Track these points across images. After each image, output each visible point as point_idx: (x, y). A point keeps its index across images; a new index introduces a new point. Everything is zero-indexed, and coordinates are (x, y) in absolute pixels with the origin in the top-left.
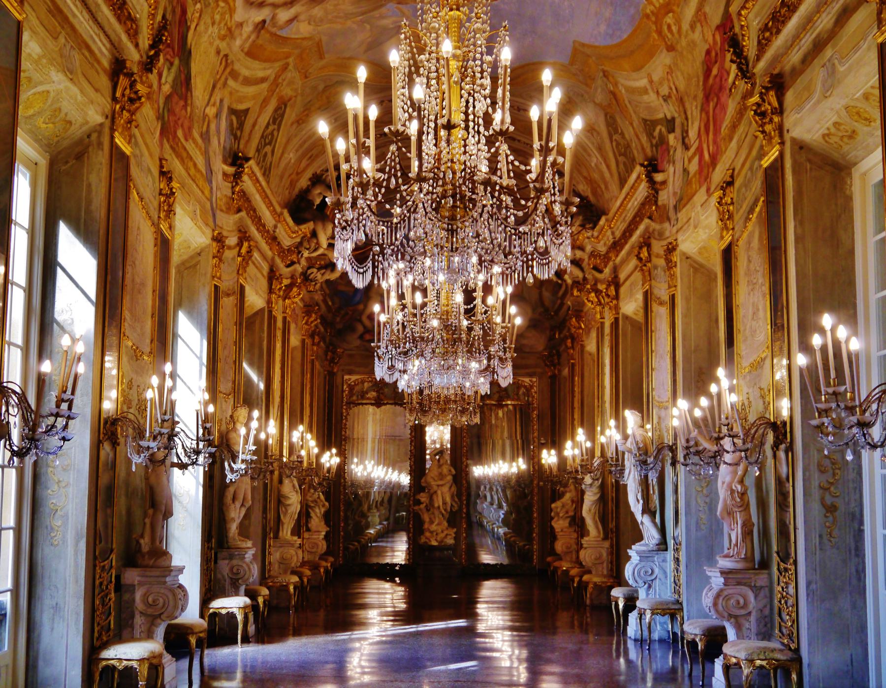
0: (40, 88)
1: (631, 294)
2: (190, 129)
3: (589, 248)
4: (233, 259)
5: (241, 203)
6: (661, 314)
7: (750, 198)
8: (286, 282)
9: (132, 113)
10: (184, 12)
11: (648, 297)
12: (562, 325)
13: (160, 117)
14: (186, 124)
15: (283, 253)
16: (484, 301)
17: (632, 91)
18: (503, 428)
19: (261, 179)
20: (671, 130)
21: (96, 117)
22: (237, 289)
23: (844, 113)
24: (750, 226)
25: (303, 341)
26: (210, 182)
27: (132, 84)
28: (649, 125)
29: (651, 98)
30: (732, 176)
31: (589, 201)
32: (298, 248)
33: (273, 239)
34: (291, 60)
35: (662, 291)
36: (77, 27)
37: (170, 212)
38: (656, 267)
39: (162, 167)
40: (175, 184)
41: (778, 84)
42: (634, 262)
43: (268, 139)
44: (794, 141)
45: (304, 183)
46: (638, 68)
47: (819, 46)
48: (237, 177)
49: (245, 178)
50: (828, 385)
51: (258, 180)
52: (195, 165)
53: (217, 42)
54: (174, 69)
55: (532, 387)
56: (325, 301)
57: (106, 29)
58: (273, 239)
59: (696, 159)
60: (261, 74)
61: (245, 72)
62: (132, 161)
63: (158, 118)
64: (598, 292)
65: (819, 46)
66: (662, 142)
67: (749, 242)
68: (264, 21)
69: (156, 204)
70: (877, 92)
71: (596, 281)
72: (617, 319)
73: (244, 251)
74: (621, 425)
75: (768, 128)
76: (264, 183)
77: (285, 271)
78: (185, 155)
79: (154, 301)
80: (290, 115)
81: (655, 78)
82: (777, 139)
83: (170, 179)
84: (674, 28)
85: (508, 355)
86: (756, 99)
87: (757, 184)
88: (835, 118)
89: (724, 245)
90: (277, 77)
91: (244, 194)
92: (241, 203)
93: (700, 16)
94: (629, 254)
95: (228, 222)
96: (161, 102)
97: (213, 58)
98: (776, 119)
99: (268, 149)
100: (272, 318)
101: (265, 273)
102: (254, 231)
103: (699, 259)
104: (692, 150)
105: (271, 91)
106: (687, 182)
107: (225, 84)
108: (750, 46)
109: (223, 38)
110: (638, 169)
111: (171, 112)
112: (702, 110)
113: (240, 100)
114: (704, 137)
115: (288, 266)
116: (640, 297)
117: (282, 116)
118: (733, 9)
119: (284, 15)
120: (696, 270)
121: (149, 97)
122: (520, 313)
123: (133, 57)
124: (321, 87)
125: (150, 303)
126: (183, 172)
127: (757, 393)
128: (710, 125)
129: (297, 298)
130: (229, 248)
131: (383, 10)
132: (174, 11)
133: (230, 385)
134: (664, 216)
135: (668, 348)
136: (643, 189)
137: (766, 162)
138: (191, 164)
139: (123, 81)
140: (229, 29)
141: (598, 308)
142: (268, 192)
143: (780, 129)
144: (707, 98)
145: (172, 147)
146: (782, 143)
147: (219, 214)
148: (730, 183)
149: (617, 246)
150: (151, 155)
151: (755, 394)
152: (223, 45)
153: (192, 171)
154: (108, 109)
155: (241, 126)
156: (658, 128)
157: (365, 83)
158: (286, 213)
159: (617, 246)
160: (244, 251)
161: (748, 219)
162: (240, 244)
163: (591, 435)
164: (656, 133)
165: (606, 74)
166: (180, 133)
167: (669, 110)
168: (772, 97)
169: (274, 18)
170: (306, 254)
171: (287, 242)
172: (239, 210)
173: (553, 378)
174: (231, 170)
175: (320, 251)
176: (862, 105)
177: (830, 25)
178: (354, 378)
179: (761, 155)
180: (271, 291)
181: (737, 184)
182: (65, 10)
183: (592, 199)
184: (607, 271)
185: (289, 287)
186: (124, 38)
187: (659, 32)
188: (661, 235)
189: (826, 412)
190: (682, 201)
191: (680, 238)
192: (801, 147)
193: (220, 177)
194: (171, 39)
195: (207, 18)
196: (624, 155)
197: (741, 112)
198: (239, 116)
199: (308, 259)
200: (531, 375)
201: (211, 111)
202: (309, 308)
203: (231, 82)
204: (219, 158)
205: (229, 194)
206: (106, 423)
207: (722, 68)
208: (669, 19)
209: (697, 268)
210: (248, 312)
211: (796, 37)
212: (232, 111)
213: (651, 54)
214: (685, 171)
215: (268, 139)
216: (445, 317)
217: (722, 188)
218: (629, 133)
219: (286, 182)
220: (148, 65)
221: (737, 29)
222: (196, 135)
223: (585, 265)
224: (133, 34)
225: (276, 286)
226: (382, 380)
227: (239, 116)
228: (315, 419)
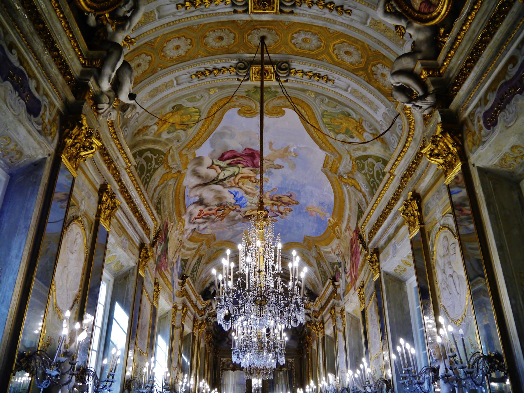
0: (113, 254)
1: (329, 327)
2: (167, 267)
3: (312, 309)
4: (180, 314)
5: (184, 293)
6: (340, 335)
7: (370, 293)
8: (200, 322)
9: (146, 262)
10: (167, 226)
11: (335, 328)
12: (303, 338)
13: (156, 263)
14: (165, 265)
15: (199, 311)
16: (273, 332)
17: (326, 252)
18: (282, 379)
19: (192, 284)
20: (340, 267)
21: (132, 264)
22: (181, 326)
23: (401, 262)
24: (371, 302)
25: (205, 345)
26: (173, 286)
27: (147, 252)
28: (332, 264)
29: (332, 255)
30: (363, 284)
31: (312, 292)
32: (204, 309)
33: (195, 306)
34: (204, 242)
35: (340, 326)
36: (129, 232)
37: (157, 297)
38: (337, 317)
39: (155, 281)
40: (160, 287)
41: (377, 252)
42: (329, 315)
43: (195, 270)
44: (384, 271)
45: (207, 285)
46: (327, 244)
47: (390, 239)
48: (183, 283)
49: (186, 284)
50: (405, 367)
51: (191, 285)
52: (168, 280)
53: (178, 236)
54: (162, 246)
55: (293, 362)
56: (214, 329)
57: (139, 233)
58: (195, 306)
59: (350, 277)
60: (193, 247)
61: (187, 246)
62: (145, 280)
63: (155, 263)
64: (316, 326)
65: (390, 239)
66: (337, 270)
67: (371, 309)
68: (195, 229)
69: (152, 295)
70: (411, 255)
71: (316, 322)
72: (324, 337)
73: (184, 311)
74: (327, 380)
75: (375, 267)
76: (193, 286)
77: (199, 318)
78: (164, 276)
79: (149, 332)
80: (203, 261)
81: (334, 248)
82: (378, 271)
83: (158, 286)
84: (339, 231)
85: (283, 352)
86: (369, 257)
87: (372, 287)
88: (398, 264)
89: (362, 309)
90: (199, 248)
91: (185, 290)
92: (184, 293)
93: (348, 228)
94: (327, 311)
95: (179, 300)
96: (157, 257)
97: (176, 242)
98: (377, 264)
99: (195, 273)
100: (194, 337)
101: (192, 319)
102: (188, 304)
103: (353, 314)
104: (348, 274)
105: (197, 252)
106: (347, 286)
107: (180, 250)
108: (366, 238)
109: (180, 235)
110: (329, 280)
111: (160, 261)
112: (351, 260)
113: (186, 256)
114: (352, 270)
115: (201, 316)
116: (332, 328)
117: (200, 261)
118: (359, 225)
119: (202, 226)
120: (352, 318)
121: (152, 256)
122: (288, 335)
123: (148, 242)
124: (215, 251)
125: (148, 333)
126: (163, 282)
127: (379, 368)
128: (354, 265)
129: (204, 329)
130: (179, 310)
131: (237, 225)
132: (163, 226)
133: (177, 364)
134: (339, 298)
135: (344, 348)
136: (331, 288)
137: (375, 279)
138: (166, 280)
139: (143, 251)
140: (183, 231)
141: (317, 332)
142: (194, 289)
143: (379, 267)
144: (352, 255)
145: (160, 274)
146: (380, 273)
147: (175, 297)
148: (363, 287)
149: (322, 308)
150: (152, 277)
151: (378, 368)
152: (180, 237)
153: (167, 282)
154: (137, 261)
155: (185, 265)
156: (336, 265)
157: (230, 256)
158: (200, 296)
159: (322, 308)
160: (184, 311)
161: (370, 300)
162: (183, 309)
163: (316, 383)
164: (335, 267)
165: (316, 247)
166: (163, 269)
167: (339, 259)
168: (375, 256)
169: (198, 227)
170: (208, 312)
171: (200, 307)
172: (183, 296)
174: (181, 281)
175: (213, 311)
176: (407, 260)
177: (393, 232)
178: (224, 359)
179: (373, 277)
180: (194, 326)
181: (365, 287)
182: (125, 227)
183: (312, 290)
184: (319, 318)
185: (201, 324)
186: (145, 236)
187: (334, 232)
188: (339, 304)
189: (405, 378)
190: (346, 293)
191: (346, 306)
192: (387, 274)
193: (177, 284)
194: (162, 235)
195: (175, 228)
196: (324, 275)
197: (365, 261)
198: (185, 261)
199: (208, 314)
200: (292, 358)
201: (175, 260)
202: (208, 332)
203: (182, 250)
204: (177, 277)
205: (180, 289)
206: (127, 382)
207: (357, 245)
208: (337, 228)
209: (353, 318)
210: (185, 334)
211: (382, 236)
212: (182, 260)
213: (331, 240)
214: (346, 281)
215: (195, 270)
216: (259, 337)
217: (360, 288)
218: (325, 267)
219: (201, 285)
220: (153, 245)
221: (361, 232)
222: (169, 268)
223: (311, 315)
224: (148, 234)
225: (196, 324)
226: (235, 362)
227: (185, 261)
228: (209, 376)
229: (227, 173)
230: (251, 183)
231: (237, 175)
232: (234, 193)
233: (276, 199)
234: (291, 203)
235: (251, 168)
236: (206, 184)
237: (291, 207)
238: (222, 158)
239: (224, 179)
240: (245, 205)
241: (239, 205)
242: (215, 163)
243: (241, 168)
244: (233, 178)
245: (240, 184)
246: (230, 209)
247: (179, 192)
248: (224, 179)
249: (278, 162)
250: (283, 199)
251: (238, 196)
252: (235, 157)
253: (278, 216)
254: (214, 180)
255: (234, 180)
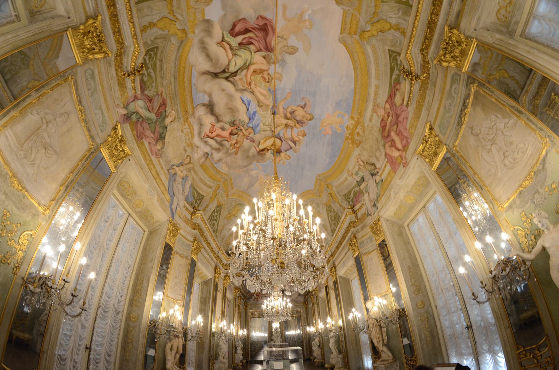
34: (221, 183)
72: (336, 278)
173: (306, 308)
180: (215, 273)
191: (381, 213)
229: (240, 62)
230: (264, 83)
231: (249, 65)
232: (246, 102)
233: (289, 115)
234: (305, 120)
235: (263, 53)
236: (215, 75)
237: (305, 128)
238: (233, 33)
239: (235, 74)
240: (258, 128)
241: (252, 128)
242: (226, 38)
243: (253, 53)
244: (245, 71)
245: (253, 85)
246: (244, 135)
247: (184, 68)
248: (235, 74)
249: (292, 41)
250: (296, 113)
251: (251, 110)
252: (247, 31)
253: (291, 148)
254: (224, 71)
255: (246, 75)
